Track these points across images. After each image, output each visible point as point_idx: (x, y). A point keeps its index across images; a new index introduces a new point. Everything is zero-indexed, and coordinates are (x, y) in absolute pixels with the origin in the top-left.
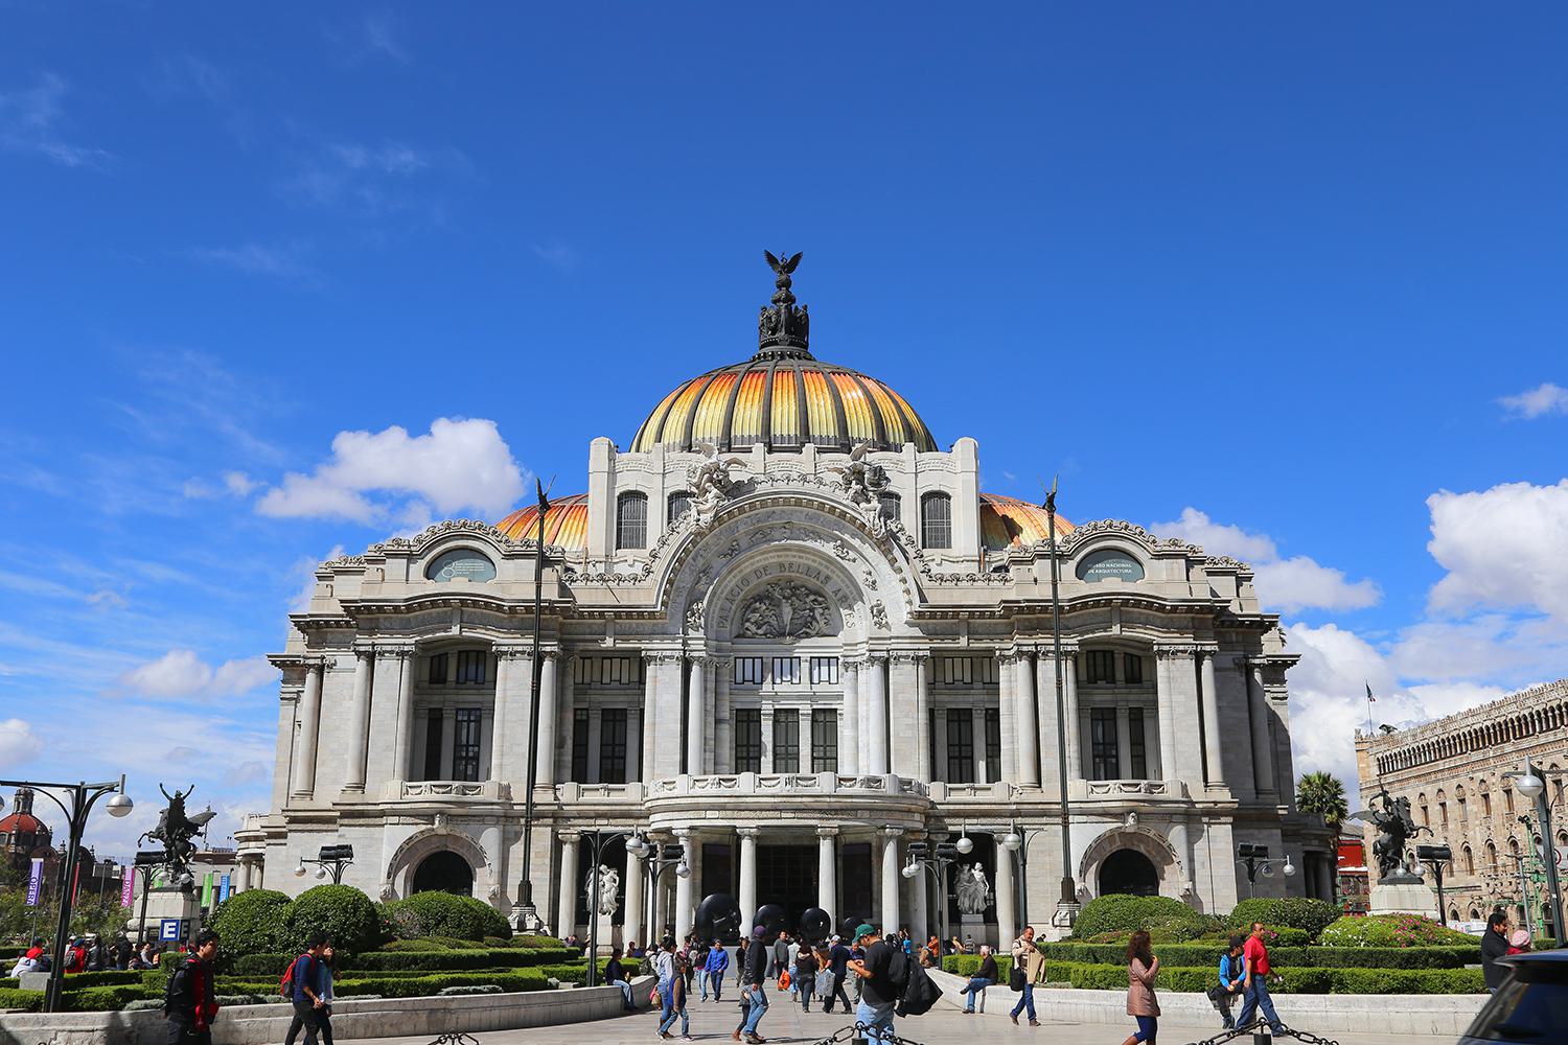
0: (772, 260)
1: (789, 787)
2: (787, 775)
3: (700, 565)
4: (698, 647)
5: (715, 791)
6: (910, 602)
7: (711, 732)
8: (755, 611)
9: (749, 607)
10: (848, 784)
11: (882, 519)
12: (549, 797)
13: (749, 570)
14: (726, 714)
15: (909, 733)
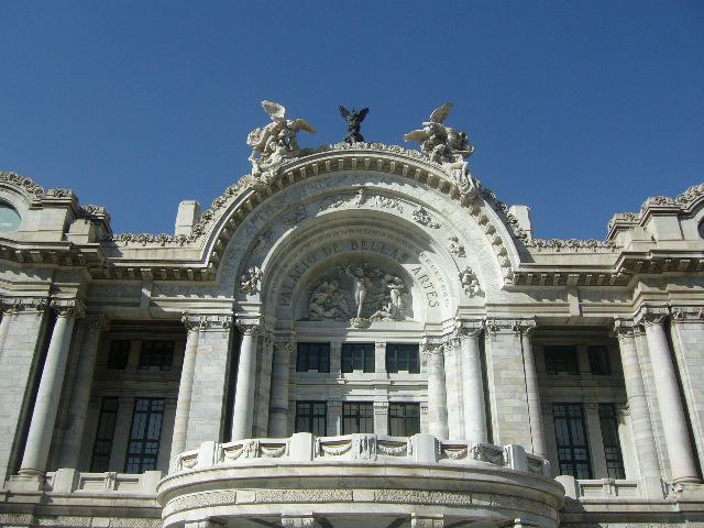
0: (344, 112)
1: (366, 453)
2: (361, 436)
3: (260, 228)
4: (252, 314)
5: (253, 460)
6: (507, 264)
7: (263, 421)
8: (323, 291)
9: (316, 287)
10: (456, 454)
11: (469, 176)
12: (33, 485)
13: (315, 246)
14: (283, 402)
15: (517, 418)
